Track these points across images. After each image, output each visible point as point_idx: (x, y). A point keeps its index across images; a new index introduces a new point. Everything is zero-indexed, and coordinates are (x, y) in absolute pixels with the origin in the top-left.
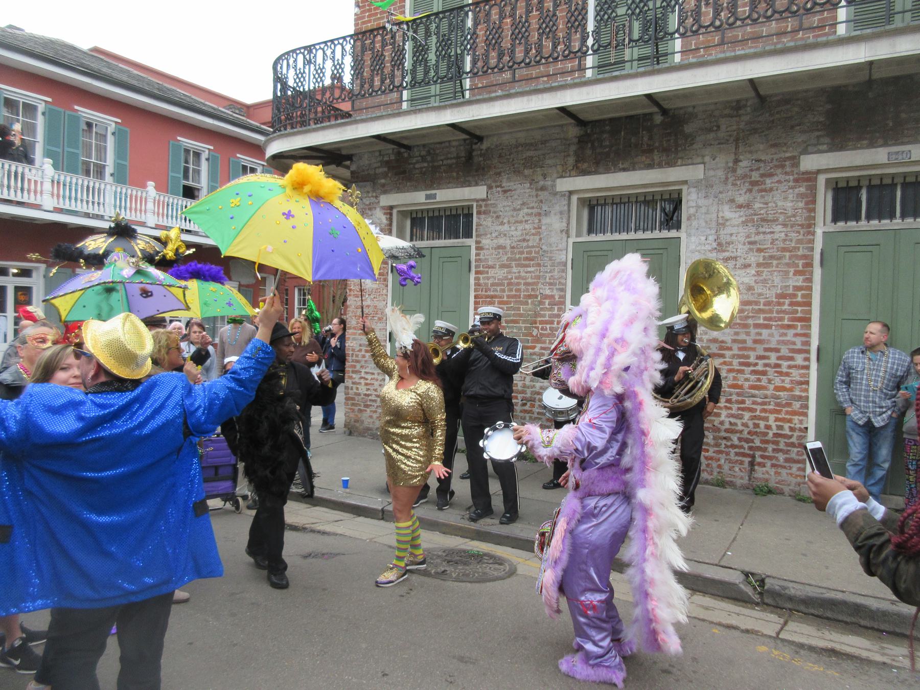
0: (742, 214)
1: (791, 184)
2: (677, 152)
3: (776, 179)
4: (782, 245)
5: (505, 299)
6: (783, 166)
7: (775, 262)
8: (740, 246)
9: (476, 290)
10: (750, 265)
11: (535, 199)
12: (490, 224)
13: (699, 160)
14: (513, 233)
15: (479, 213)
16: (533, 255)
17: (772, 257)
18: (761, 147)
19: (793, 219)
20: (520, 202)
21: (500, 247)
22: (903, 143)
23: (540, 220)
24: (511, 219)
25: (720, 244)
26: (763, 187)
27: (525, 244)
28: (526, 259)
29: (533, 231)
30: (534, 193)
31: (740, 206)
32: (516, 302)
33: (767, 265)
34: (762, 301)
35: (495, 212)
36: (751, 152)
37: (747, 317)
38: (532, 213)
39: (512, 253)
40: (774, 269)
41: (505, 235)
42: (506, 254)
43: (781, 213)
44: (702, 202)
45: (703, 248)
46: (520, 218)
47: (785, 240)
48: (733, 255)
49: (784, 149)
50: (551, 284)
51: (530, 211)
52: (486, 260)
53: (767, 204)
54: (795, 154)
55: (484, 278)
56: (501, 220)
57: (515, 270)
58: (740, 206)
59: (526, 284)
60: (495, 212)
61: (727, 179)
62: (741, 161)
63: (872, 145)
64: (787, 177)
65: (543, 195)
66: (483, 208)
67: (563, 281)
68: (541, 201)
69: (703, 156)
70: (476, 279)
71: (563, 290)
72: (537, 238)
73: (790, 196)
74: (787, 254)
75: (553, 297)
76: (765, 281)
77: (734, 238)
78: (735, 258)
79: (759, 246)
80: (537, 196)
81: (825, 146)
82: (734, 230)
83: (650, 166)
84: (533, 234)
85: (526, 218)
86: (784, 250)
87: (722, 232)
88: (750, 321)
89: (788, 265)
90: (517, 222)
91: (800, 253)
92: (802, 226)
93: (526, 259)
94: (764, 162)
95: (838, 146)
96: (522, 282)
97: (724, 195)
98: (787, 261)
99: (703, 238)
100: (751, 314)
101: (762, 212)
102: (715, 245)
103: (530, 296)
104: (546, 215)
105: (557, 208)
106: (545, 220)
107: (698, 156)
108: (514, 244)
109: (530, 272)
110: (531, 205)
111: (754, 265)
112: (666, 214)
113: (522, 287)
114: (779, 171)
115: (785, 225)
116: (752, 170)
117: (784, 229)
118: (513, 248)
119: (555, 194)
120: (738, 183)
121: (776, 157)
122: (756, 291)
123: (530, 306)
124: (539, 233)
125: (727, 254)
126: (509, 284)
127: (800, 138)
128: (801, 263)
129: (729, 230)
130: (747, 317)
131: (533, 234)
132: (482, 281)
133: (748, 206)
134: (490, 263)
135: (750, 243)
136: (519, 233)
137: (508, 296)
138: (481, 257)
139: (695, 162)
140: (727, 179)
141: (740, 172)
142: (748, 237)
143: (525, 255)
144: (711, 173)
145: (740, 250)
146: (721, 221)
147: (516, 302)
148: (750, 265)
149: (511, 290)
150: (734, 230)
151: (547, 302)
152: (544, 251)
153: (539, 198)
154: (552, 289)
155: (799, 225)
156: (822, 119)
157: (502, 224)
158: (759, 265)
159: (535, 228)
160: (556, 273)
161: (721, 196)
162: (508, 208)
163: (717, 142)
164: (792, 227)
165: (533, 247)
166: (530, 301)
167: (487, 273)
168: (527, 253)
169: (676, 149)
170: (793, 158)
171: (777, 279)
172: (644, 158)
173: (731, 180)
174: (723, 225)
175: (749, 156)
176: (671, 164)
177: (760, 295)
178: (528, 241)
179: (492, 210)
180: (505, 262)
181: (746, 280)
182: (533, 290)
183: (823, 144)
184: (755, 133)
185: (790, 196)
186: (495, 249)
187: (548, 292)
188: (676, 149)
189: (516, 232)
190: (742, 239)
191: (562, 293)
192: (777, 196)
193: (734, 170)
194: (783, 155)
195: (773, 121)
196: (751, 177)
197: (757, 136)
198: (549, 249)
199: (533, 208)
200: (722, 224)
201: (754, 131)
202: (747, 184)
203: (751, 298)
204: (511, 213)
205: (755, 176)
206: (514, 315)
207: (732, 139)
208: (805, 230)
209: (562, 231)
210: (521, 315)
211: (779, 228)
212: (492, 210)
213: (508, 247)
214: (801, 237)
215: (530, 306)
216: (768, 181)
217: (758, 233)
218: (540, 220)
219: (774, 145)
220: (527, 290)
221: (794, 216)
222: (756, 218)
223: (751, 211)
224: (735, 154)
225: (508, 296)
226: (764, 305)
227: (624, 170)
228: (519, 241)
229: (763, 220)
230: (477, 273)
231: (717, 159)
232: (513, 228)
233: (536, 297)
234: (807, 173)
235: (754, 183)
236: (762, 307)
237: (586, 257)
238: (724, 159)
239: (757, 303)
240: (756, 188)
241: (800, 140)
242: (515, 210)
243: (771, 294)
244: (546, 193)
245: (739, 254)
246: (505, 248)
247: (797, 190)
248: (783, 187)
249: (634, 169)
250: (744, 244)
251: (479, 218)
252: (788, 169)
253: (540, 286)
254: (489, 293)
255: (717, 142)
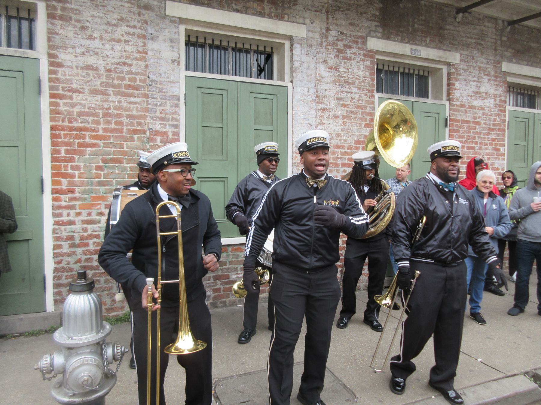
0: (332, 74)
1: (362, 57)
2: (283, 8)
3: (353, 51)
4: (357, 103)
5: (101, 133)
6: (357, 42)
7: (353, 116)
8: (332, 101)
9: (52, 119)
10: (338, 117)
11: (137, 18)
12: (71, 35)
13: (301, 20)
14: (108, 53)
15: (51, 16)
16: (138, 83)
17: (351, 112)
18: (344, 23)
19: (363, 84)
20: (116, 16)
21: (88, 67)
22: (416, 44)
23: (145, 44)
24: (104, 35)
25: (318, 97)
26: (345, 55)
27: (126, 69)
28: (129, 87)
29: (138, 55)
30: (135, 9)
31: (331, 68)
32: (117, 137)
33: (349, 118)
34: (346, 145)
35: (78, 21)
36: (337, 25)
37: (338, 158)
38: (133, 34)
39: (108, 77)
40: (353, 121)
41: (96, 53)
42: (99, 77)
43: (357, 78)
44: (304, 58)
45: (306, 98)
46: (117, 36)
47: (359, 100)
48: (327, 107)
49: (357, 29)
50: (162, 119)
51: (131, 30)
52: (67, 81)
53: (348, 69)
54: (364, 35)
55: (65, 104)
56: (89, 33)
57: (113, 98)
58: (331, 68)
59: (130, 117)
60: (78, 21)
61: (322, 43)
62: (331, 30)
63: (402, 41)
64: (360, 52)
65: (147, 15)
66: (59, 12)
67: (176, 116)
68: (146, 22)
69: (304, 18)
70: (51, 104)
71: (177, 127)
72: (143, 64)
73: (362, 66)
74: (361, 111)
75: (165, 133)
76: (347, 130)
77: (327, 92)
78: (328, 110)
79: (343, 102)
80: (140, 14)
81: (379, 35)
82: (327, 87)
83: (261, 14)
84: (137, 59)
85: (126, 38)
86: (359, 107)
87: (319, 87)
88: (339, 162)
89: (360, 118)
90: (113, 40)
91: (367, 111)
92: (368, 90)
93: (129, 87)
94: (345, 35)
95: (386, 37)
96: (125, 113)
97: (320, 55)
98: (360, 115)
99: (306, 90)
100: (340, 156)
101: (345, 75)
102: (314, 97)
103: (135, 132)
104: (152, 39)
105: (166, 33)
106: (151, 45)
107: (300, 17)
108: (112, 67)
109: (135, 103)
110: (133, 23)
111: (341, 117)
112: (259, 66)
113: (125, 120)
114: (355, 45)
115: (359, 89)
116: (338, 40)
117: (358, 91)
118: (109, 71)
119: (164, 17)
120: (330, 48)
121: (353, 33)
122: (342, 138)
123: (136, 143)
124: (144, 59)
125: (323, 106)
126: (105, 115)
127: (367, 24)
128: (368, 118)
129: (324, 86)
130: (338, 158)
131: (137, 59)
132: (62, 108)
133: (336, 68)
134: (74, 86)
135: (339, 99)
136: (117, 54)
137: (105, 130)
138: (59, 76)
139: (298, 21)
140: (322, 43)
141: (330, 39)
142: (337, 94)
143: (127, 82)
144: (311, 35)
145: (331, 103)
146: (318, 78)
147: (117, 137)
148: (338, 117)
149: (109, 123)
150: (327, 87)
151: (158, 139)
152: (152, 81)
153: (142, 17)
154: (165, 125)
155: (367, 90)
156: (378, 14)
157: (91, 38)
158: (344, 117)
159: (139, 52)
160: (168, 108)
161: (318, 56)
162: (98, 20)
163: (313, 9)
164: (363, 90)
165: (138, 73)
166: (136, 137)
167: (71, 98)
168: (130, 80)
169: (283, 5)
170: (362, 37)
171: (355, 130)
172: (255, 5)
173: (325, 44)
174: (320, 81)
175: (336, 27)
176: (280, 18)
177: (345, 141)
178: (130, 65)
179: (74, 17)
180: (98, 87)
181: (336, 128)
182: (139, 124)
183: (377, 32)
184: (339, 10)
185: (362, 66)
186: (82, 68)
187: (159, 128)
188: (283, 5)
189: (114, 53)
190: (333, 95)
191: (176, 130)
192: (353, 64)
193: (327, 37)
194: (356, 33)
195: (350, 4)
196: (337, 46)
197: (340, 13)
198: (158, 79)
199: (135, 27)
200: (319, 80)
201: (339, 9)
202: (335, 51)
203: (340, 143)
204: (105, 27)
205: (340, 45)
206: (114, 153)
207: (324, 10)
208: (370, 94)
209: (173, 61)
210: (125, 153)
211: (355, 90)
212: (74, 17)
213: (102, 69)
214: (368, 99)
215: (136, 143)
216: (348, 51)
217: (343, 92)
218: (145, 44)
219: (351, 24)
220: (132, 124)
221: (364, 82)
222: (341, 79)
223: (337, 73)
224: (327, 24)
225: (105, 130)
226: (348, 149)
227: (238, 11)
228: (117, 64)
229: (346, 82)
230: (52, 96)
231: (315, 23)
232: (108, 47)
233: (144, 132)
234: (370, 51)
235: (340, 51)
236: (346, 150)
237: (200, 94)
238: (319, 25)
239: (343, 147)
240: (341, 55)
241: (366, 25)
242: (109, 24)
243: (351, 140)
244: (151, 14)
245: (331, 107)
246: (97, 69)
247: (365, 63)
248: (357, 58)
249: (246, 13)
250: (334, 99)
251: (52, 24)
252: (360, 46)
253: (148, 120)
254: (74, 124)
255: (313, 9)
